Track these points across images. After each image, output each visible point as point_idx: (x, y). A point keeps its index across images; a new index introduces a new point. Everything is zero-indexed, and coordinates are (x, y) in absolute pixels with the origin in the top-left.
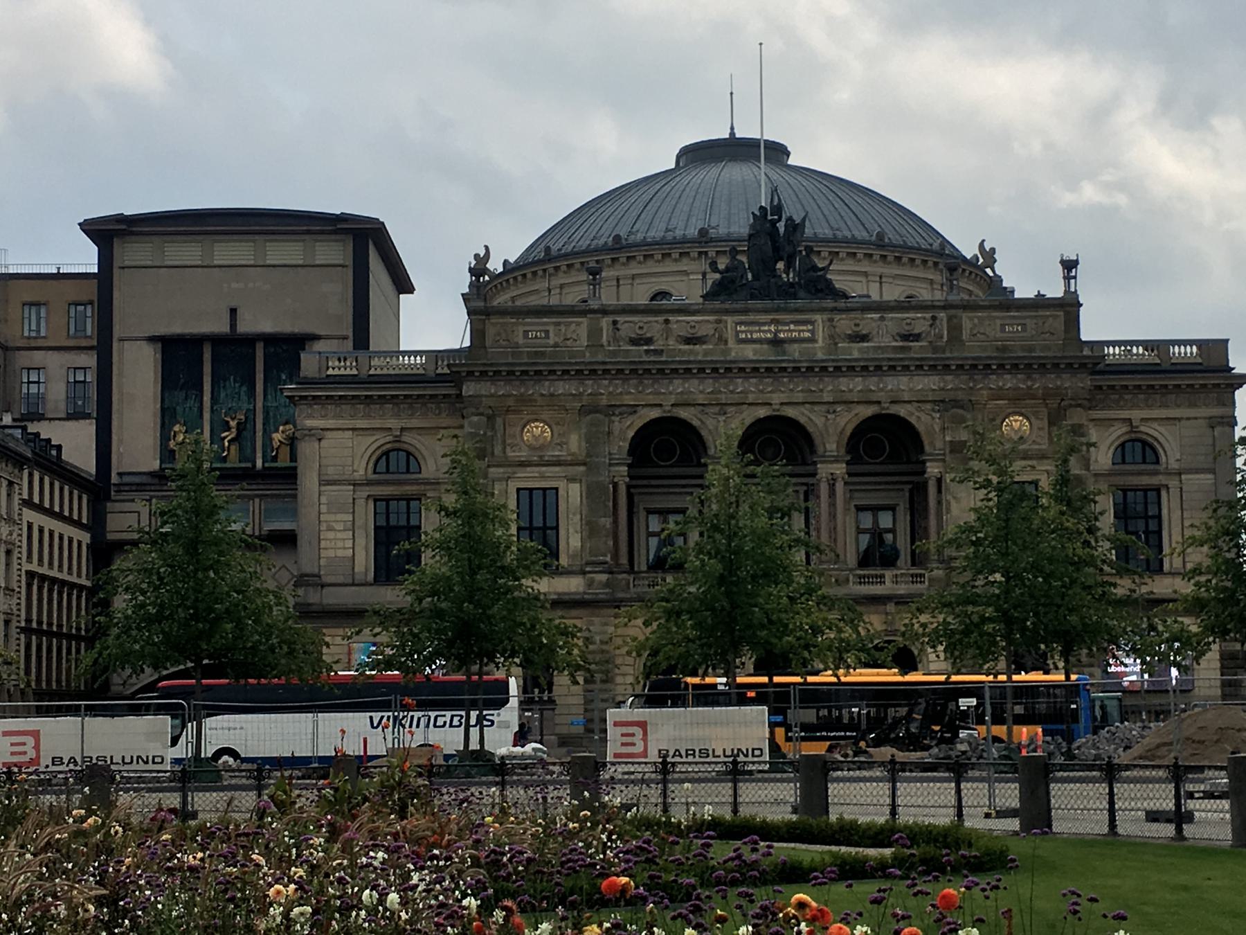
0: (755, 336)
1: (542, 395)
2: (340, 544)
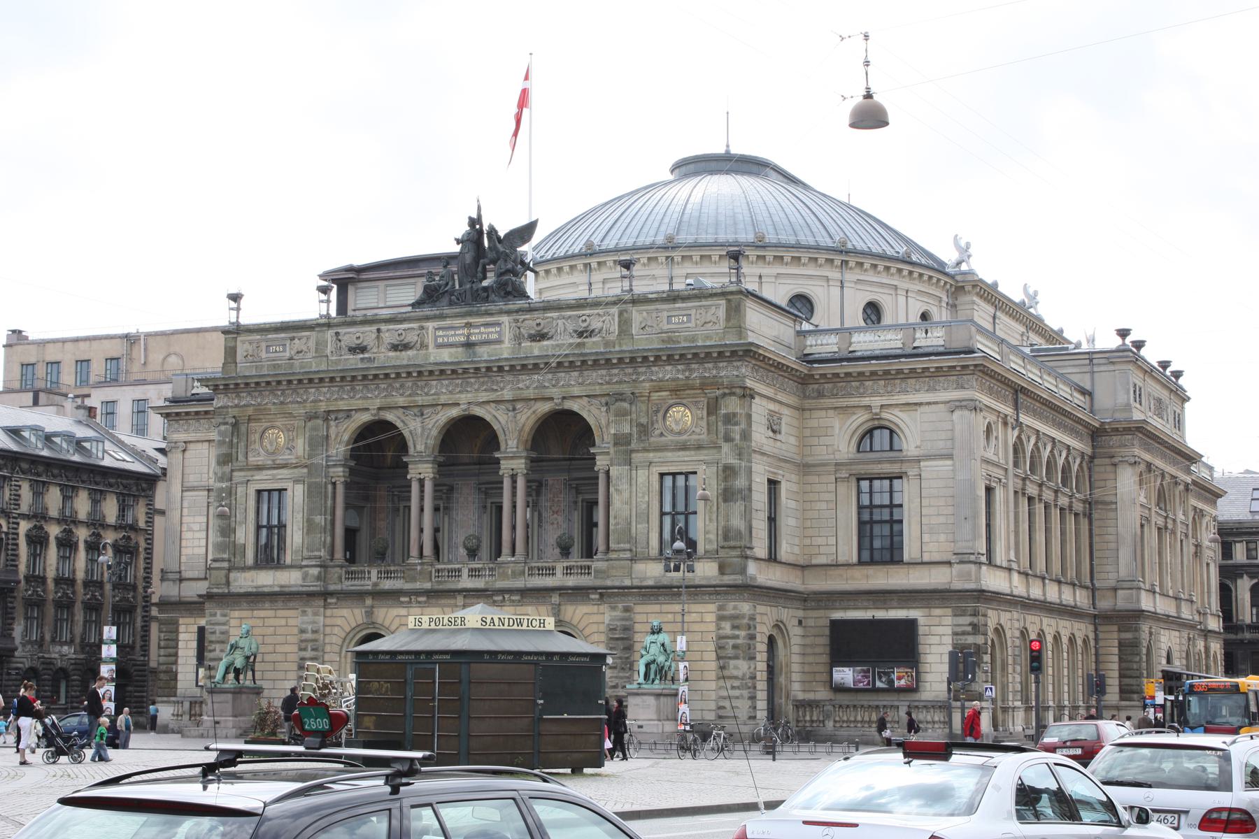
0: (451, 340)
1: (274, 403)
2: (196, 543)
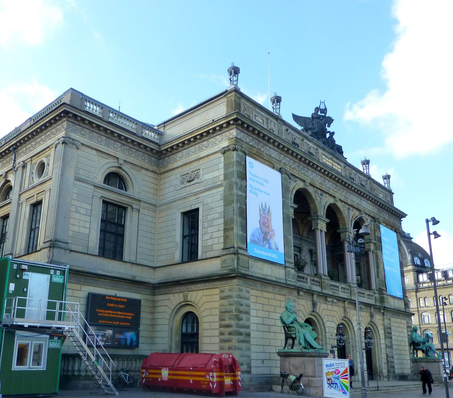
1: (267, 154)
2: (82, 224)
